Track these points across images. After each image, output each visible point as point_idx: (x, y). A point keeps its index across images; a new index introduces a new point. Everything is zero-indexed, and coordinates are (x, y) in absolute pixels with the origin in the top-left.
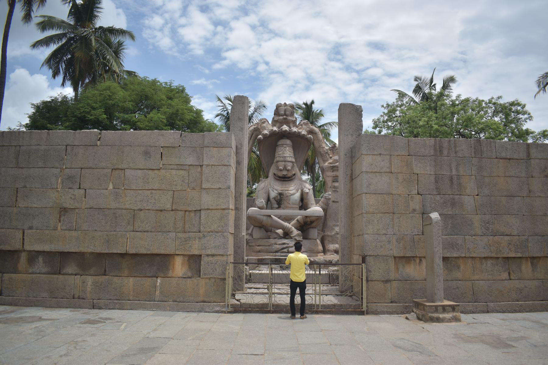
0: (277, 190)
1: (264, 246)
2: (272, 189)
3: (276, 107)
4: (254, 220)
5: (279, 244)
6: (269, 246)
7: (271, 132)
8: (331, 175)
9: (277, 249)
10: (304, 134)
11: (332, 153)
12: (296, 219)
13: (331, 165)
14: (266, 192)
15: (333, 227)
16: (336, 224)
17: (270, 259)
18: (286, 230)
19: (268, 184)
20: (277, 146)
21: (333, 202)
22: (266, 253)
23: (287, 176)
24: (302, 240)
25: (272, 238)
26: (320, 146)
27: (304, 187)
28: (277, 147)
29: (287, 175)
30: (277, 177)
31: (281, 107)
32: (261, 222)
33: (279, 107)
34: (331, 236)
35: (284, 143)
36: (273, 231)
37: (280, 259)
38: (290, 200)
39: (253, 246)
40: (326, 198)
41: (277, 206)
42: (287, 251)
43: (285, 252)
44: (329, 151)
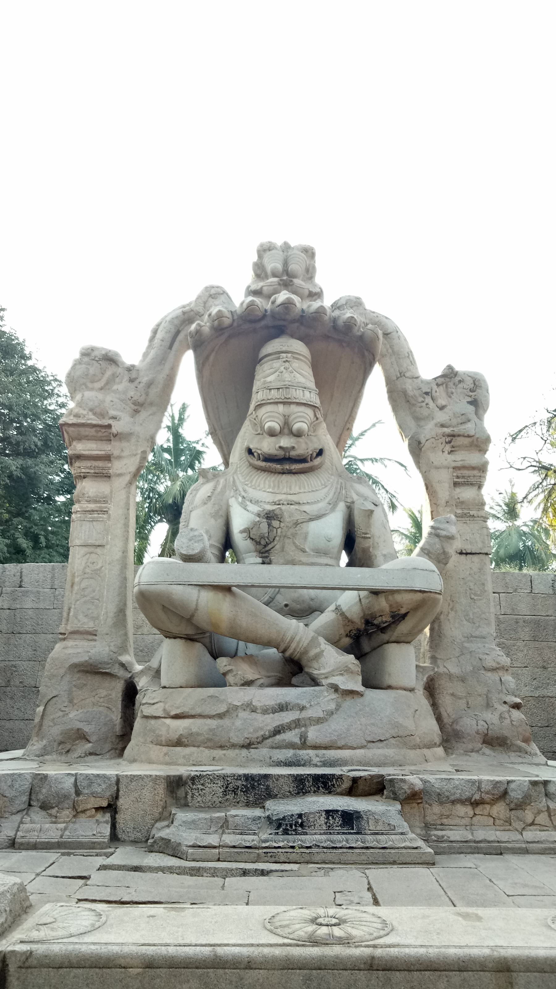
0: (257, 502)
1: (201, 716)
2: (240, 499)
3: (258, 251)
4: (164, 608)
5: (265, 711)
6: (220, 716)
7: (239, 312)
8: (445, 463)
9: (256, 731)
10: (352, 317)
11: (444, 395)
12: (332, 607)
13: (446, 429)
14: (217, 512)
15: (466, 645)
16: (477, 633)
17: (224, 777)
18: (293, 646)
19: (225, 487)
20: (261, 360)
21: (461, 553)
22: (206, 751)
23: (293, 453)
24: (361, 688)
25: (236, 685)
26: (402, 375)
27: (355, 497)
28: (258, 367)
29: (293, 448)
30: (259, 459)
31: (273, 251)
32: (192, 616)
33: (265, 251)
34: (463, 679)
35: (284, 349)
36: (241, 653)
37: (266, 777)
38: (305, 538)
39: (159, 717)
40: (438, 536)
41: (260, 560)
42: (297, 740)
43: (292, 746)
44: (435, 387)
